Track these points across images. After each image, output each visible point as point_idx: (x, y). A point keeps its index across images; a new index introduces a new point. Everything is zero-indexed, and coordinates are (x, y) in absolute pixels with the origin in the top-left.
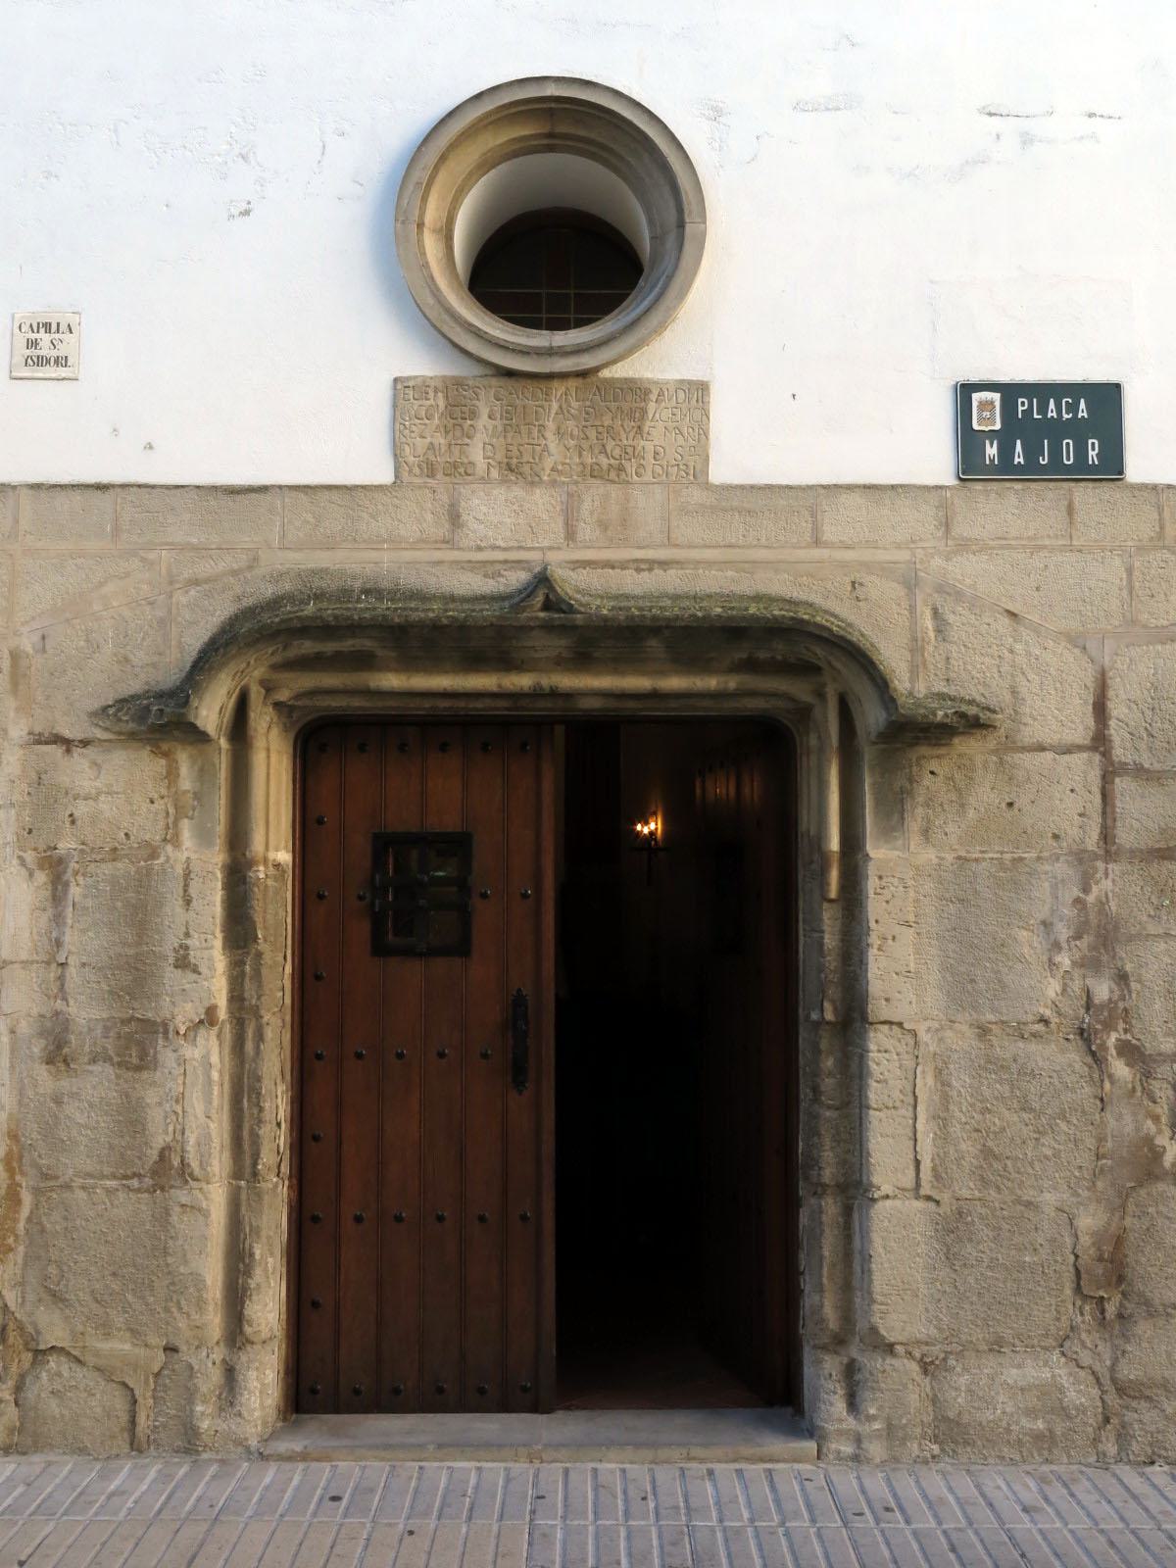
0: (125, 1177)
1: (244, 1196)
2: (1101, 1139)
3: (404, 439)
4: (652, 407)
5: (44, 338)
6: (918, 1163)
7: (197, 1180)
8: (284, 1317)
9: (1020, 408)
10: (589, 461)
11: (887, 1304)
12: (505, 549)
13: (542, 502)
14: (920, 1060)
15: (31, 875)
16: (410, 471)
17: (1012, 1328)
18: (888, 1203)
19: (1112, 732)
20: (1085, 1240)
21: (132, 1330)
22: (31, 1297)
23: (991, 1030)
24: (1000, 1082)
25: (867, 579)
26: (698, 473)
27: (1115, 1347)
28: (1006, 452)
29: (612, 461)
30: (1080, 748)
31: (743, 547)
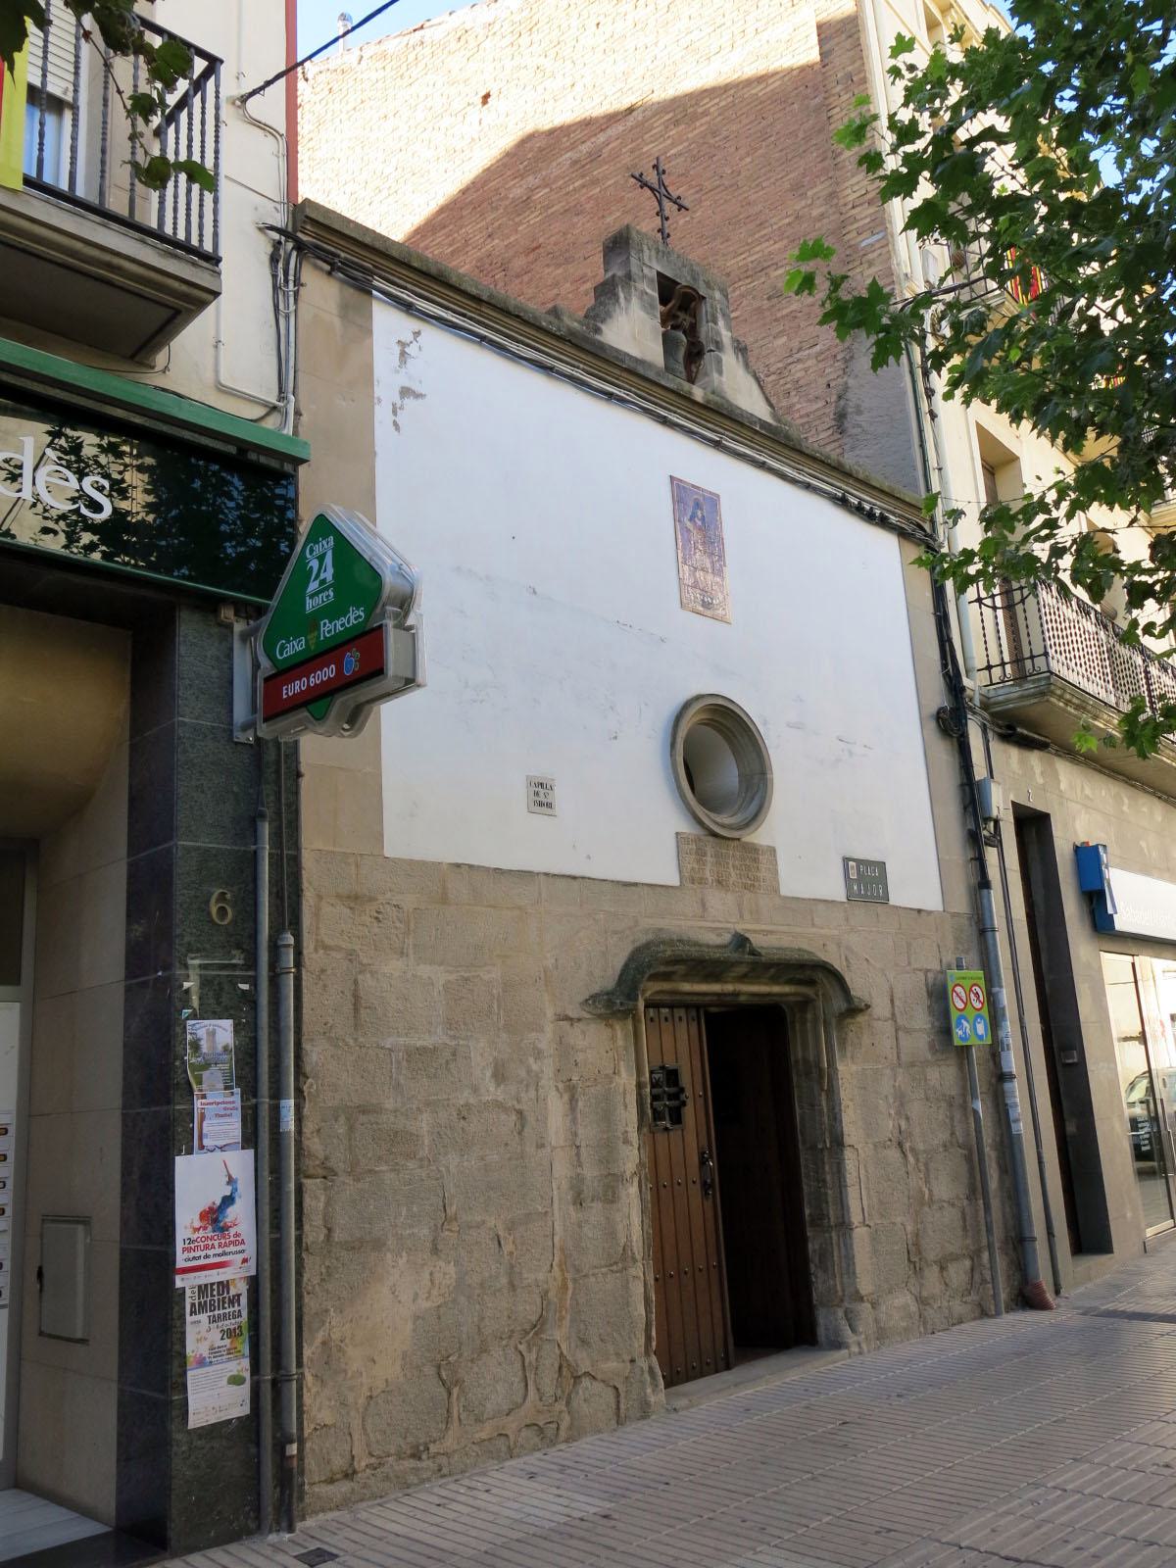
0: (611, 1265)
5: (542, 791)
22: (573, 1345)
26: (776, 890)
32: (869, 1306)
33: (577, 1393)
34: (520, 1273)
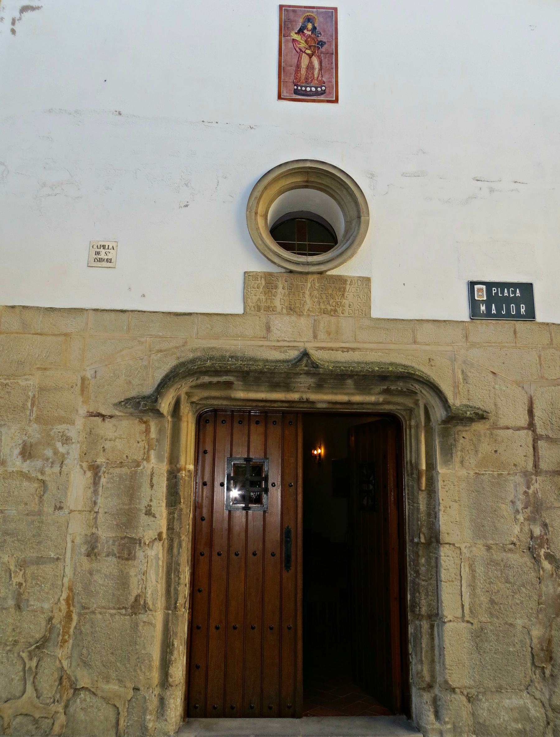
0: (119, 609)
1: (170, 618)
2: (540, 596)
3: (248, 296)
4: (348, 287)
5: (103, 251)
6: (463, 606)
7: (151, 610)
8: (185, 673)
9: (494, 292)
10: (323, 307)
11: (452, 670)
12: (289, 342)
13: (304, 322)
14: (463, 560)
15: (85, 472)
16: (250, 309)
17: (506, 681)
18: (451, 624)
19: (536, 422)
20: (535, 641)
21: (119, 680)
22: (74, 664)
23: (492, 548)
24: (496, 570)
27: (550, 690)
28: (489, 308)
29: (332, 308)
30: (523, 428)
31: (386, 343)
32: (464, 699)
33: (75, 702)
34: (28, 600)
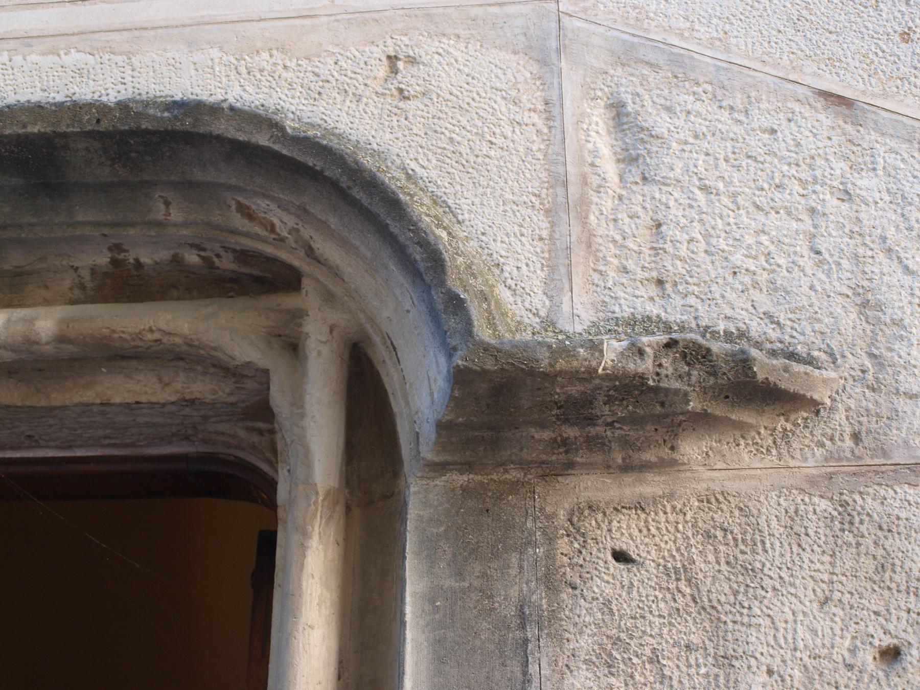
25: (426, 48)
